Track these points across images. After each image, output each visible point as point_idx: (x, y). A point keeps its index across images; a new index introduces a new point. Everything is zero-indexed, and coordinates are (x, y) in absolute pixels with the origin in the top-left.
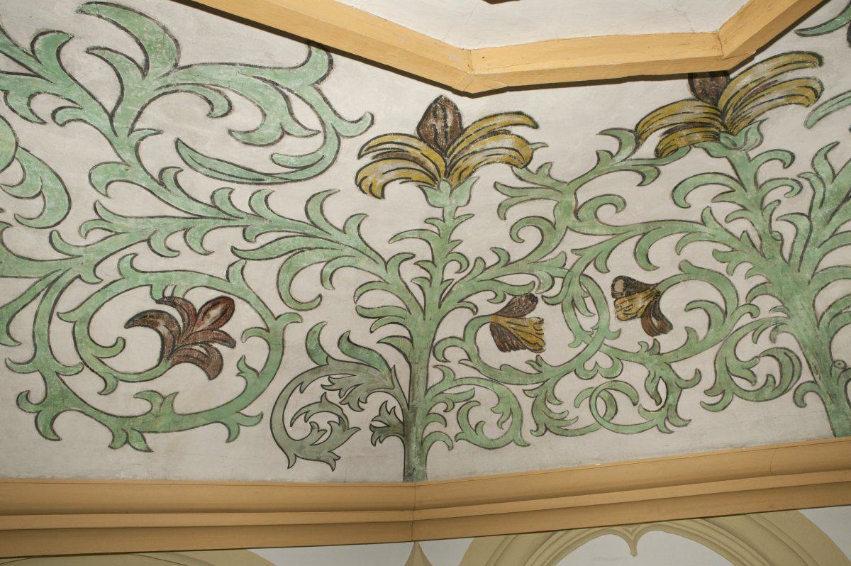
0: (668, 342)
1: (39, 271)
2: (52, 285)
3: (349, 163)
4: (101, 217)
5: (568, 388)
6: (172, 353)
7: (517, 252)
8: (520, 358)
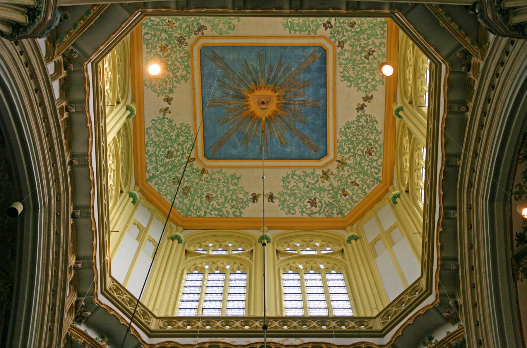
0: (360, 186)
1: (299, 198)
2: (301, 199)
3: (320, 179)
4: (304, 192)
5: (354, 197)
6: (312, 205)
7: (339, 184)
8: (347, 197)
